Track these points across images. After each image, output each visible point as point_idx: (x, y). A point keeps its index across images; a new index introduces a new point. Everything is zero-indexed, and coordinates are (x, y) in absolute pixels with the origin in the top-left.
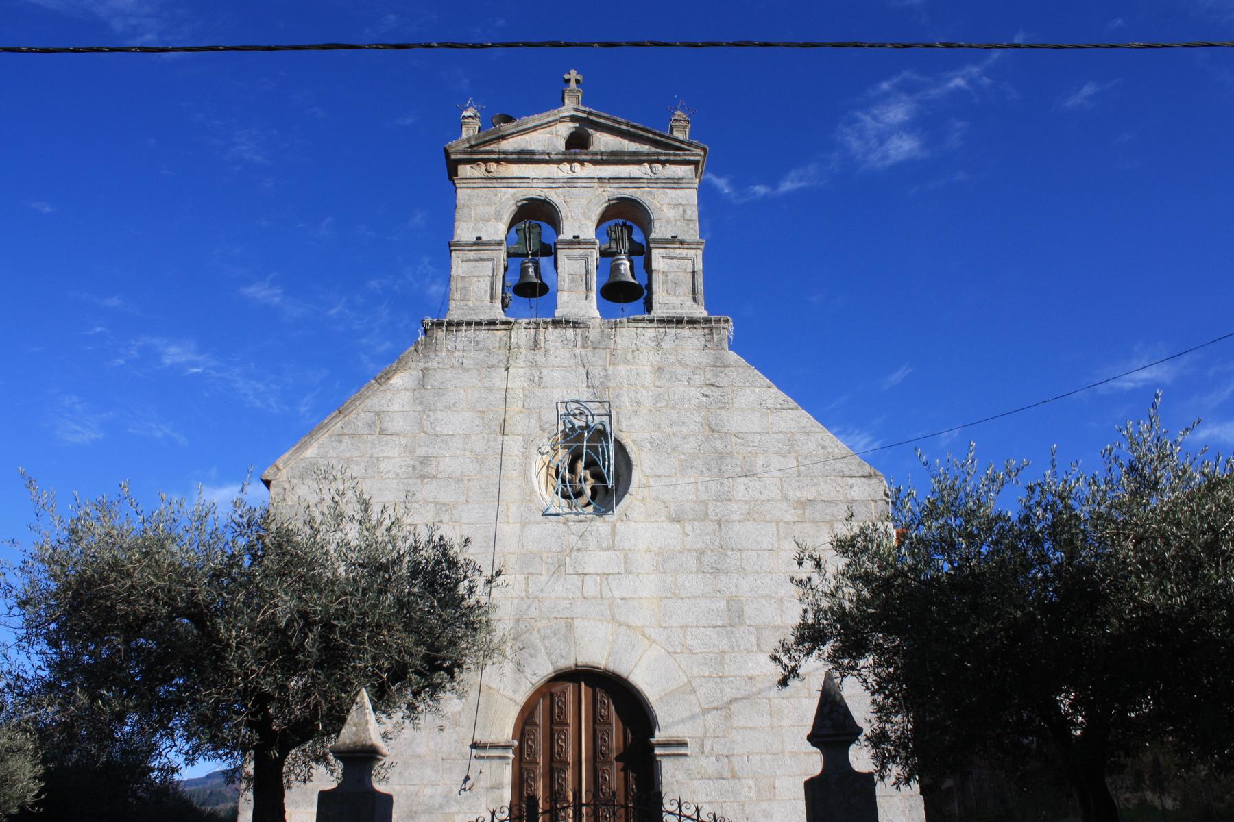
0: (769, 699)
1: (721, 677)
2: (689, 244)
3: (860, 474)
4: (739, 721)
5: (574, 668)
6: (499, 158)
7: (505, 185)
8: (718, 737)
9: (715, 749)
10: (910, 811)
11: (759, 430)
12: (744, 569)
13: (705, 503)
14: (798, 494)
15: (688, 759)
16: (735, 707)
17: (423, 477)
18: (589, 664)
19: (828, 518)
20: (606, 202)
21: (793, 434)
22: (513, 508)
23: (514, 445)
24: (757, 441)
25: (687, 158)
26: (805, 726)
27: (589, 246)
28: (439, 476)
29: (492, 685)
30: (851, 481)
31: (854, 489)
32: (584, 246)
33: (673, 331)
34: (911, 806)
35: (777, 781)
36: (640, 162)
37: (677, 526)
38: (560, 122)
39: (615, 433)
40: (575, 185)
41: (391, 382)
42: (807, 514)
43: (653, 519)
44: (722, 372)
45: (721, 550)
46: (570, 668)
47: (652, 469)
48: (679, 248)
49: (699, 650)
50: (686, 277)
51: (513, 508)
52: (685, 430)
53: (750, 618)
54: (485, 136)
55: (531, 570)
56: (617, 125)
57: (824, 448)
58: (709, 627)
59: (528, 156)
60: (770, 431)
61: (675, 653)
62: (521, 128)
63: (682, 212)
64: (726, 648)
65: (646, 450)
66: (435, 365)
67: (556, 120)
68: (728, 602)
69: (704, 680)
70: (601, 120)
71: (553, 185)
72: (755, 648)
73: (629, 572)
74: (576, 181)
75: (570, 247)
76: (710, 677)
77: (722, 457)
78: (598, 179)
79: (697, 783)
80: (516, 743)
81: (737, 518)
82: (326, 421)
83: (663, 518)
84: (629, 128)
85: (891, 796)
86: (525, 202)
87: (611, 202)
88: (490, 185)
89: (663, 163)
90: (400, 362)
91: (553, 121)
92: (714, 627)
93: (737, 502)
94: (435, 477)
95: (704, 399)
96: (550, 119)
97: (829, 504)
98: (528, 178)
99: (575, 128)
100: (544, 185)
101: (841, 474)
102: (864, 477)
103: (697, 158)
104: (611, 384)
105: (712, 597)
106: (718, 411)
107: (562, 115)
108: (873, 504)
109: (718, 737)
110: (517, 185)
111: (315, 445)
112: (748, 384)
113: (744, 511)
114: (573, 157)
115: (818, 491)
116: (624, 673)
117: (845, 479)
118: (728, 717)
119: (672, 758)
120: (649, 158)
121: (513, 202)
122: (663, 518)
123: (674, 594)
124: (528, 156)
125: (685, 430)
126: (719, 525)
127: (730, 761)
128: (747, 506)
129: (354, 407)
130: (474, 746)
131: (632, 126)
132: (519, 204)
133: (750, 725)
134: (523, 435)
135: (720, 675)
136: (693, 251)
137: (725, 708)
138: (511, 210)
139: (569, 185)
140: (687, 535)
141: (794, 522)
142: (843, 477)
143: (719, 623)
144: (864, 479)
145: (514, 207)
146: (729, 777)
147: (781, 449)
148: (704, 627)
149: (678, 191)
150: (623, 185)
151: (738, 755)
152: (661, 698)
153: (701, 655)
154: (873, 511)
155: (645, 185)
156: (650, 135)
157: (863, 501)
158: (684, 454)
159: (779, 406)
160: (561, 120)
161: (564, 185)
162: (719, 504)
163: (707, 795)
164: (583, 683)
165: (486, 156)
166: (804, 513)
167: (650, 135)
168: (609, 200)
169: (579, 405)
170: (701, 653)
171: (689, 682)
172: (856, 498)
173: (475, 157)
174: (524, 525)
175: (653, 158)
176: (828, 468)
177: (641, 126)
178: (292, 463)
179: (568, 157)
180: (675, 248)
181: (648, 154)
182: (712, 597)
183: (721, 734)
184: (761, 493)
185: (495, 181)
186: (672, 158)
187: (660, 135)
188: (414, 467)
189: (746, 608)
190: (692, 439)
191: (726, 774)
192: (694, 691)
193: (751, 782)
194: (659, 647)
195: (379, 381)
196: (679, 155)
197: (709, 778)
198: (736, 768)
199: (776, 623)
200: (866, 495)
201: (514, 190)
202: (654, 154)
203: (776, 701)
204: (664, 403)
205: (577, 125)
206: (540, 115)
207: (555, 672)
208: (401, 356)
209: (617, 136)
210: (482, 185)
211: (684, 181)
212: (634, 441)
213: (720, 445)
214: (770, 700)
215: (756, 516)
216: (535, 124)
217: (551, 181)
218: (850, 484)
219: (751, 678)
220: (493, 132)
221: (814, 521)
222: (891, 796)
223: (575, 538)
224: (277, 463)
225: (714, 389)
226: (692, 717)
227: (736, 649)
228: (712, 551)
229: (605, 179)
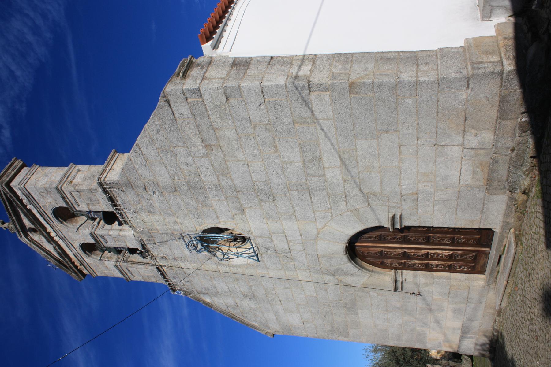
0: (359, 173)
1: (346, 196)
2: (62, 195)
3: (169, 108)
4: (377, 189)
5: (348, 255)
6: (71, 264)
7: (83, 261)
8: (388, 200)
9: (397, 202)
10: (452, 88)
11: (164, 168)
12: (266, 181)
13: (226, 197)
14: (201, 148)
15: (403, 214)
16: (365, 190)
17: (254, 296)
18: (344, 249)
19: (211, 131)
20: (63, 224)
21: (157, 148)
22: (260, 271)
23: (222, 269)
24: (172, 169)
25: (9, 192)
26: (379, 153)
27: (94, 235)
28: (252, 292)
29: (361, 283)
30: (177, 115)
31: (182, 113)
32: (96, 237)
33: (122, 206)
34: (447, 87)
35: (421, 171)
36: (30, 211)
37: (247, 211)
38: (32, 239)
39: (199, 233)
40: (63, 236)
41: (210, 302)
42: (214, 144)
43: (246, 221)
44: (135, 184)
45: (256, 191)
46: (347, 256)
47: (214, 220)
48: (68, 198)
49: (328, 205)
50: (83, 195)
51: (260, 271)
52: (182, 204)
53: (301, 180)
54: (63, 269)
55: (293, 268)
56: (15, 221)
57: (158, 131)
58: (311, 199)
59: (62, 254)
60: (161, 161)
61: (332, 216)
62: (49, 256)
63: (44, 194)
64: (325, 192)
65: (203, 221)
66: (194, 290)
67: (33, 243)
68: (291, 190)
69: (348, 204)
70: (18, 226)
71: (70, 245)
72: (323, 178)
73: (284, 232)
74: (61, 237)
75: (100, 242)
76: (346, 201)
77: (192, 187)
78: (52, 228)
79: (420, 211)
80: (393, 271)
81: (231, 182)
82: (239, 322)
83: (244, 216)
84: (13, 215)
85: (438, 101)
86: (87, 252)
87: (62, 221)
88: (88, 266)
89: (21, 201)
90: (199, 300)
91: (35, 244)
92: (311, 197)
93: (219, 181)
94: (253, 293)
95: (157, 193)
96: (35, 246)
97: (201, 130)
98: (74, 254)
99: (31, 232)
100: (73, 248)
101: (174, 120)
102: (170, 105)
103: (5, 187)
104: (170, 232)
105: (290, 197)
106: (162, 187)
107: (29, 242)
108: (189, 100)
109: (388, 200)
110: (80, 256)
111: (251, 323)
112: (135, 171)
113: (225, 178)
114: (48, 238)
115: (193, 136)
116: (349, 237)
117: (177, 118)
118: (374, 194)
119: (403, 221)
120: (23, 208)
121: (90, 258)
122: (244, 216)
123: (292, 214)
124: (62, 254)
125: (182, 204)
126: (239, 191)
127: (405, 195)
128: (221, 177)
129: (228, 313)
130: (396, 289)
131: (10, 215)
132: (89, 254)
133: (379, 183)
134: (217, 265)
135: (344, 196)
136: (65, 192)
137: (367, 198)
138: (95, 257)
139: (65, 239)
140: (251, 206)
141: (222, 151)
142: (176, 120)
143: (307, 195)
144: (172, 105)
145: (93, 256)
146: (417, 196)
147: (171, 156)
148: (312, 202)
149: (33, 195)
150: (48, 218)
151: (401, 191)
152: (363, 224)
153: (332, 205)
154: (196, 100)
155: (41, 209)
156: (9, 207)
157: (190, 107)
158: (198, 205)
159: (141, 156)
160: (32, 240)
161: (67, 241)
162: (224, 190)
163: (429, 207)
164: (356, 244)
165: (74, 268)
166: (214, 145)
167: (9, 207)
168: (62, 223)
169: (189, 245)
170: (330, 204)
171: (350, 211)
172: (189, 111)
173: (77, 272)
174: (267, 268)
175: (21, 207)
176: (173, 129)
177: (7, 213)
178: (263, 329)
179: (50, 240)
180: (69, 200)
181: (21, 209)
182: (290, 197)
183: (386, 199)
184: (208, 169)
185: (84, 265)
186: (15, 198)
187: (5, 204)
188: (250, 299)
189: (294, 181)
190: (186, 201)
191: (415, 197)
192: (356, 210)
193: (421, 185)
194: (330, 222)
195: (211, 306)
196: (10, 196)
197: (417, 205)
198: (411, 192)
199: (302, 166)
200: (184, 104)
201: (84, 258)
202: (19, 207)
203: (361, 169)
204: (170, 212)
205: (29, 232)
206: (36, 251)
207: (351, 262)
208: (196, 301)
209: (21, 218)
210: (89, 268)
211: (24, 193)
212: (200, 225)
213: (184, 188)
214: (360, 172)
215: (226, 172)
216: (43, 252)
217: (68, 246)
218: (179, 115)
219: (345, 181)
220: (59, 266)
221: (217, 139)
222: (438, 101)
223: (269, 251)
224: (264, 334)
225: (147, 189)
226: (373, 210)
227: (325, 188)
228: (258, 196)
229: (50, 226)
